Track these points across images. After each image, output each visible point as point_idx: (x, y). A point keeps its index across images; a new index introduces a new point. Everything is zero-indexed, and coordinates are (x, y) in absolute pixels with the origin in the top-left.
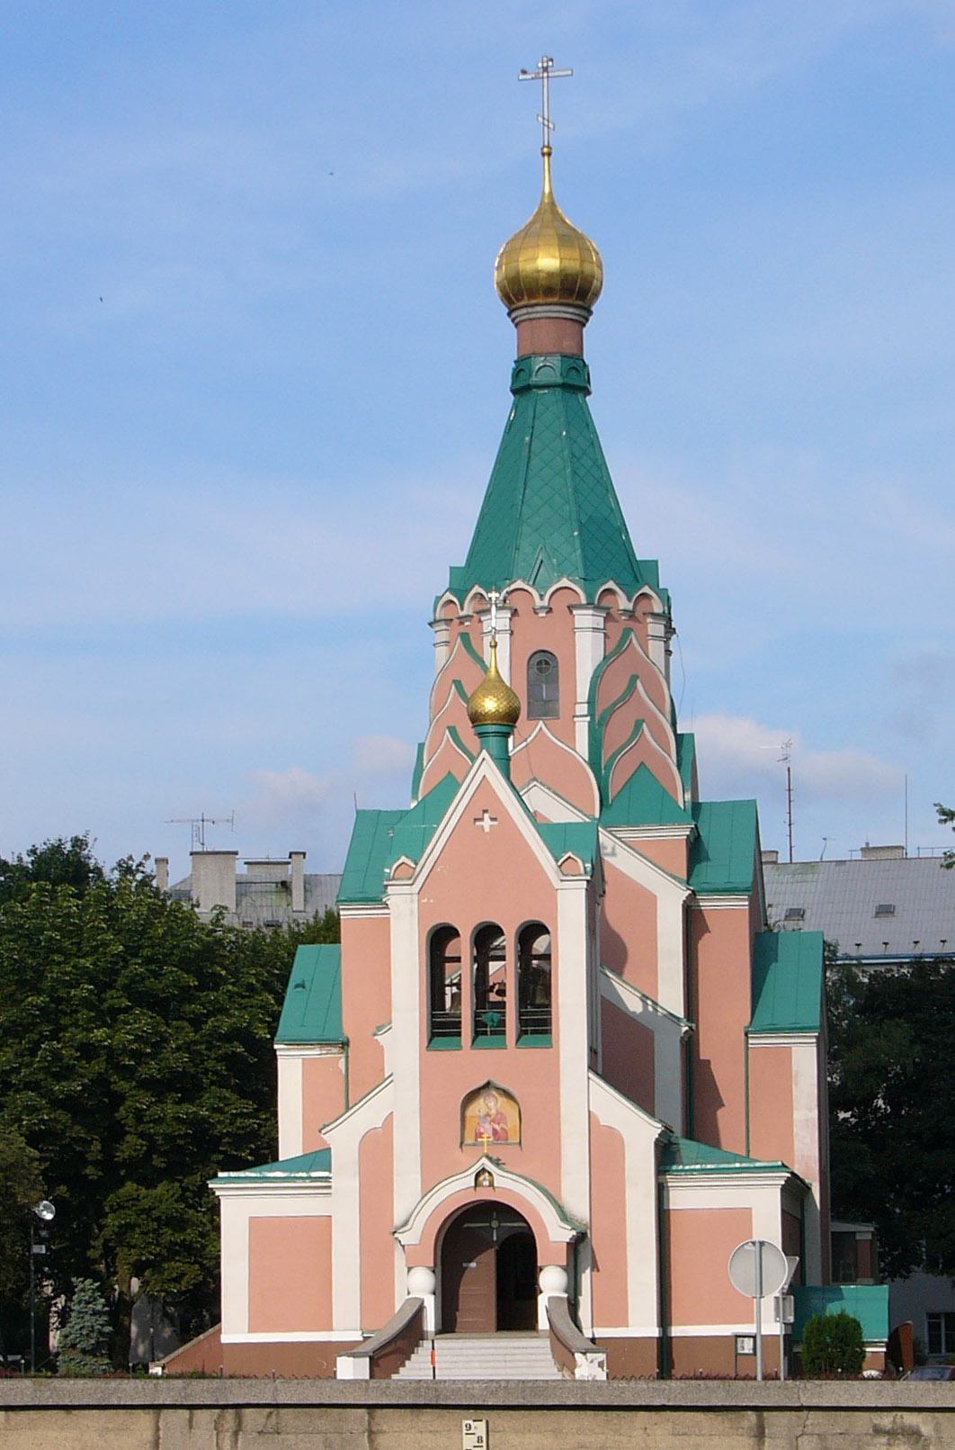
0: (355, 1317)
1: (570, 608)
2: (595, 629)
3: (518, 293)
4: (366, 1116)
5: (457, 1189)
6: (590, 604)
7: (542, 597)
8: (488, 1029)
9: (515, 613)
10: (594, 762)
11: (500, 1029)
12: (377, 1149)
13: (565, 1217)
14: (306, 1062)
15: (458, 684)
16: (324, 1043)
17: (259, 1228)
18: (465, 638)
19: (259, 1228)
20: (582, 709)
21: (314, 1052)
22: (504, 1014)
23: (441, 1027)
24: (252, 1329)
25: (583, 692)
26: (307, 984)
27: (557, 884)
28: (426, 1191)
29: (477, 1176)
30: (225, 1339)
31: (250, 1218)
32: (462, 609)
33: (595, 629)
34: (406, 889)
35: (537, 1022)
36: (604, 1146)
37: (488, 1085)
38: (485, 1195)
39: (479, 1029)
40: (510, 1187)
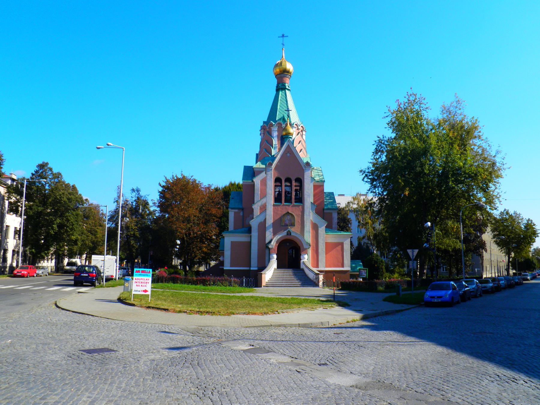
0: (256, 265)
8: (288, 200)
14: (235, 213)
16: (239, 209)
17: (233, 243)
19: (233, 243)
21: (237, 210)
23: (278, 199)
24: (231, 266)
27: (304, 169)
30: (225, 268)
34: (271, 169)
35: (300, 199)
38: (288, 237)
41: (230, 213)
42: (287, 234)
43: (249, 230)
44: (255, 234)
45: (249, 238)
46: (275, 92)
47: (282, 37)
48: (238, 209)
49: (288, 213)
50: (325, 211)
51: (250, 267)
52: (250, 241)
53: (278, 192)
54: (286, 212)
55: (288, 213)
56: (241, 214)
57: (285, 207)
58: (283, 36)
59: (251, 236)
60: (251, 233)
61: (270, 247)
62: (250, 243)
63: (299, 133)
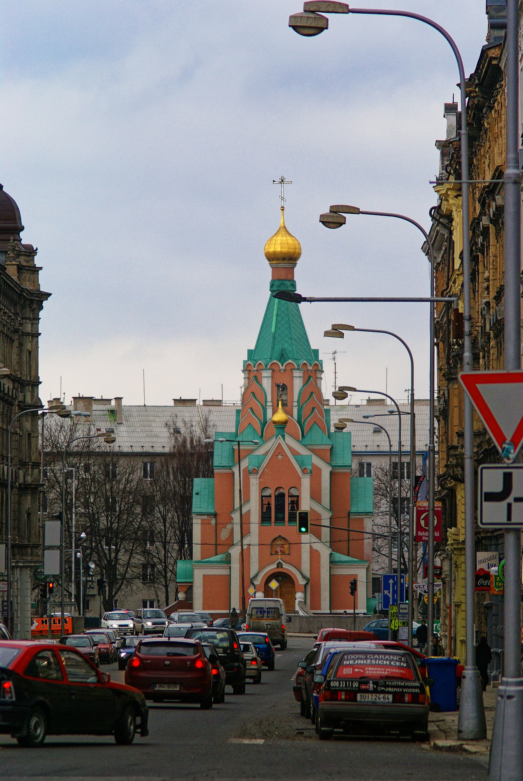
1: (292, 370)
2: (300, 377)
3: (272, 257)
6: (298, 369)
7: (282, 365)
8: (280, 519)
9: (273, 371)
10: (299, 422)
11: (283, 519)
13: (304, 577)
15: (253, 393)
18: (256, 377)
20: (295, 404)
21: (206, 517)
22: (284, 515)
23: (265, 518)
24: (204, 609)
25: (296, 398)
26: (200, 493)
27: (301, 476)
28: (261, 568)
29: (278, 564)
31: (204, 575)
32: (254, 367)
33: (300, 377)
34: (255, 477)
36: (314, 555)
37: (280, 536)
38: (280, 570)
39: (276, 519)
41: (194, 521)
42: (278, 567)
43: (228, 561)
45: (229, 570)
47: (281, 183)
48: (208, 515)
49: (280, 536)
50: (352, 517)
52: (229, 574)
53: (267, 506)
54: (278, 536)
56: (213, 522)
59: (230, 567)
60: (230, 564)
61: (256, 583)
63: (309, 377)
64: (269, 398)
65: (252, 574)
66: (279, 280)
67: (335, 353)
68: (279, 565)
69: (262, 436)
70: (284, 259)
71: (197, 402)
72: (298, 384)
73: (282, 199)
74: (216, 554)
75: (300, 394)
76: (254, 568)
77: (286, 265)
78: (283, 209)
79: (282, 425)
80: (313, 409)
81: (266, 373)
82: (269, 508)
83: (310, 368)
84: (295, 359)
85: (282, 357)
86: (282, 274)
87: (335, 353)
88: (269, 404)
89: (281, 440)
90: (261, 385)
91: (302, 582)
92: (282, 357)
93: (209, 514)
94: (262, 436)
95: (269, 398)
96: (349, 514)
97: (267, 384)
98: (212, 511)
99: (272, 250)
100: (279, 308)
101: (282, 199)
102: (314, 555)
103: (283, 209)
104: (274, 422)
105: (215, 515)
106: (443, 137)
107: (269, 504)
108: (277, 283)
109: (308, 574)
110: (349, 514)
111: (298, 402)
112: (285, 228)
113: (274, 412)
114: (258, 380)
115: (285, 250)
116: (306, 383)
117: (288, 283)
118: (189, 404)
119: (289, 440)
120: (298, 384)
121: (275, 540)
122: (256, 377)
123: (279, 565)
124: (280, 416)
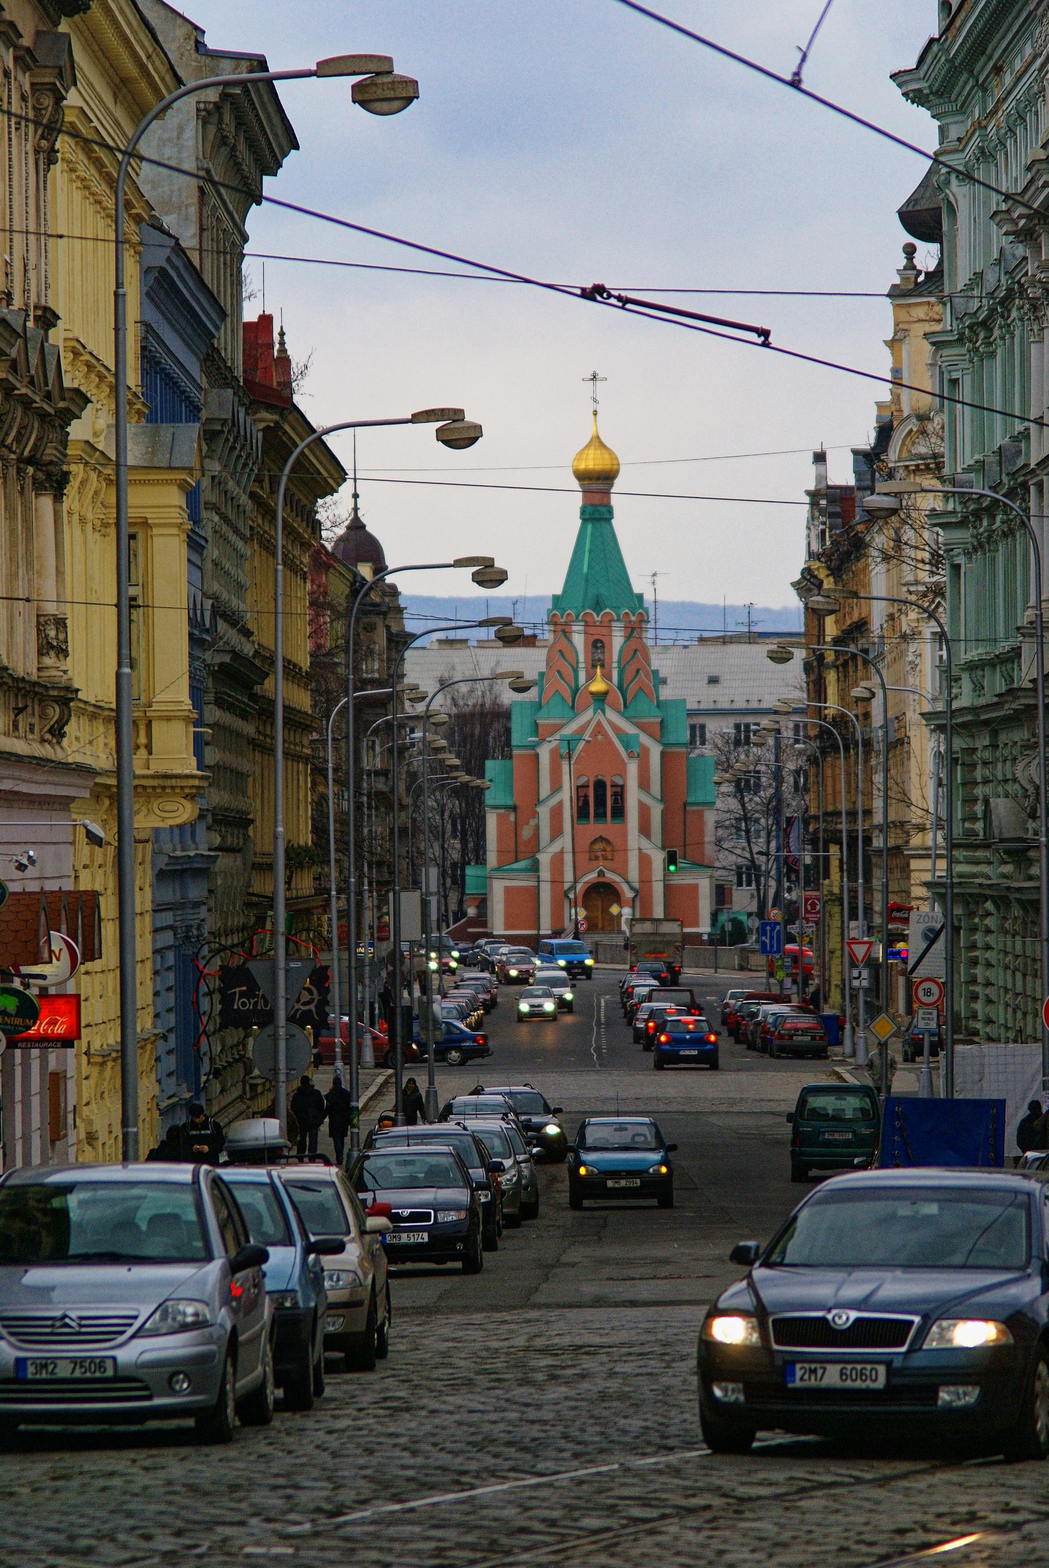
3: (582, 476)
4: (556, 847)
5: (592, 877)
8: (600, 815)
10: (620, 687)
11: (605, 815)
12: (557, 861)
13: (632, 888)
14: (498, 815)
19: (508, 890)
20: (615, 665)
21: (502, 811)
23: (582, 813)
24: (506, 929)
25: (615, 658)
35: (619, 812)
36: (645, 861)
38: (602, 880)
40: (610, 876)
43: (535, 867)
44: (545, 874)
46: (578, 522)
51: (539, 929)
55: (601, 839)
56: (512, 818)
57: (593, 828)
58: (594, 377)
62: (536, 891)
64: (582, 658)
65: (566, 886)
66: (592, 505)
67: (655, 575)
68: (601, 874)
69: (573, 707)
70: (598, 479)
71: (470, 643)
72: (618, 641)
73: (595, 400)
74: (517, 861)
75: (621, 652)
76: (569, 876)
77: (601, 487)
78: (595, 413)
79: (601, 698)
80: (638, 671)
81: (578, 628)
82: (586, 802)
83: (633, 618)
84: (615, 608)
85: (598, 605)
86: (597, 498)
87: (655, 575)
88: (582, 665)
89: (600, 716)
90: (571, 642)
91: (629, 894)
92: (598, 605)
93: (506, 807)
94: (573, 707)
95: (582, 658)
96: (685, 805)
97: (578, 640)
98: (510, 803)
99: (582, 466)
100: (592, 542)
101: (595, 400)
102: (645, 861)
103: (595, 413)
104: (591, 693)
105: (514, 808)
106: (812, 487)
107: (586, 796)
108: (589, 509)
109: (637, 885)
110: (685, 805)
111: (619, 662)
112: (598, 437)
113: (590, 677)
114: (567, 634)
115: (598, 467)
116: (628, 638)
117: (603, 509)
118: (458, 646)
119: (611, 714)
120: (618, 641)
121: (594, 842)
122: (564, 632)
123: (601, 874)
124: (598, 686)
